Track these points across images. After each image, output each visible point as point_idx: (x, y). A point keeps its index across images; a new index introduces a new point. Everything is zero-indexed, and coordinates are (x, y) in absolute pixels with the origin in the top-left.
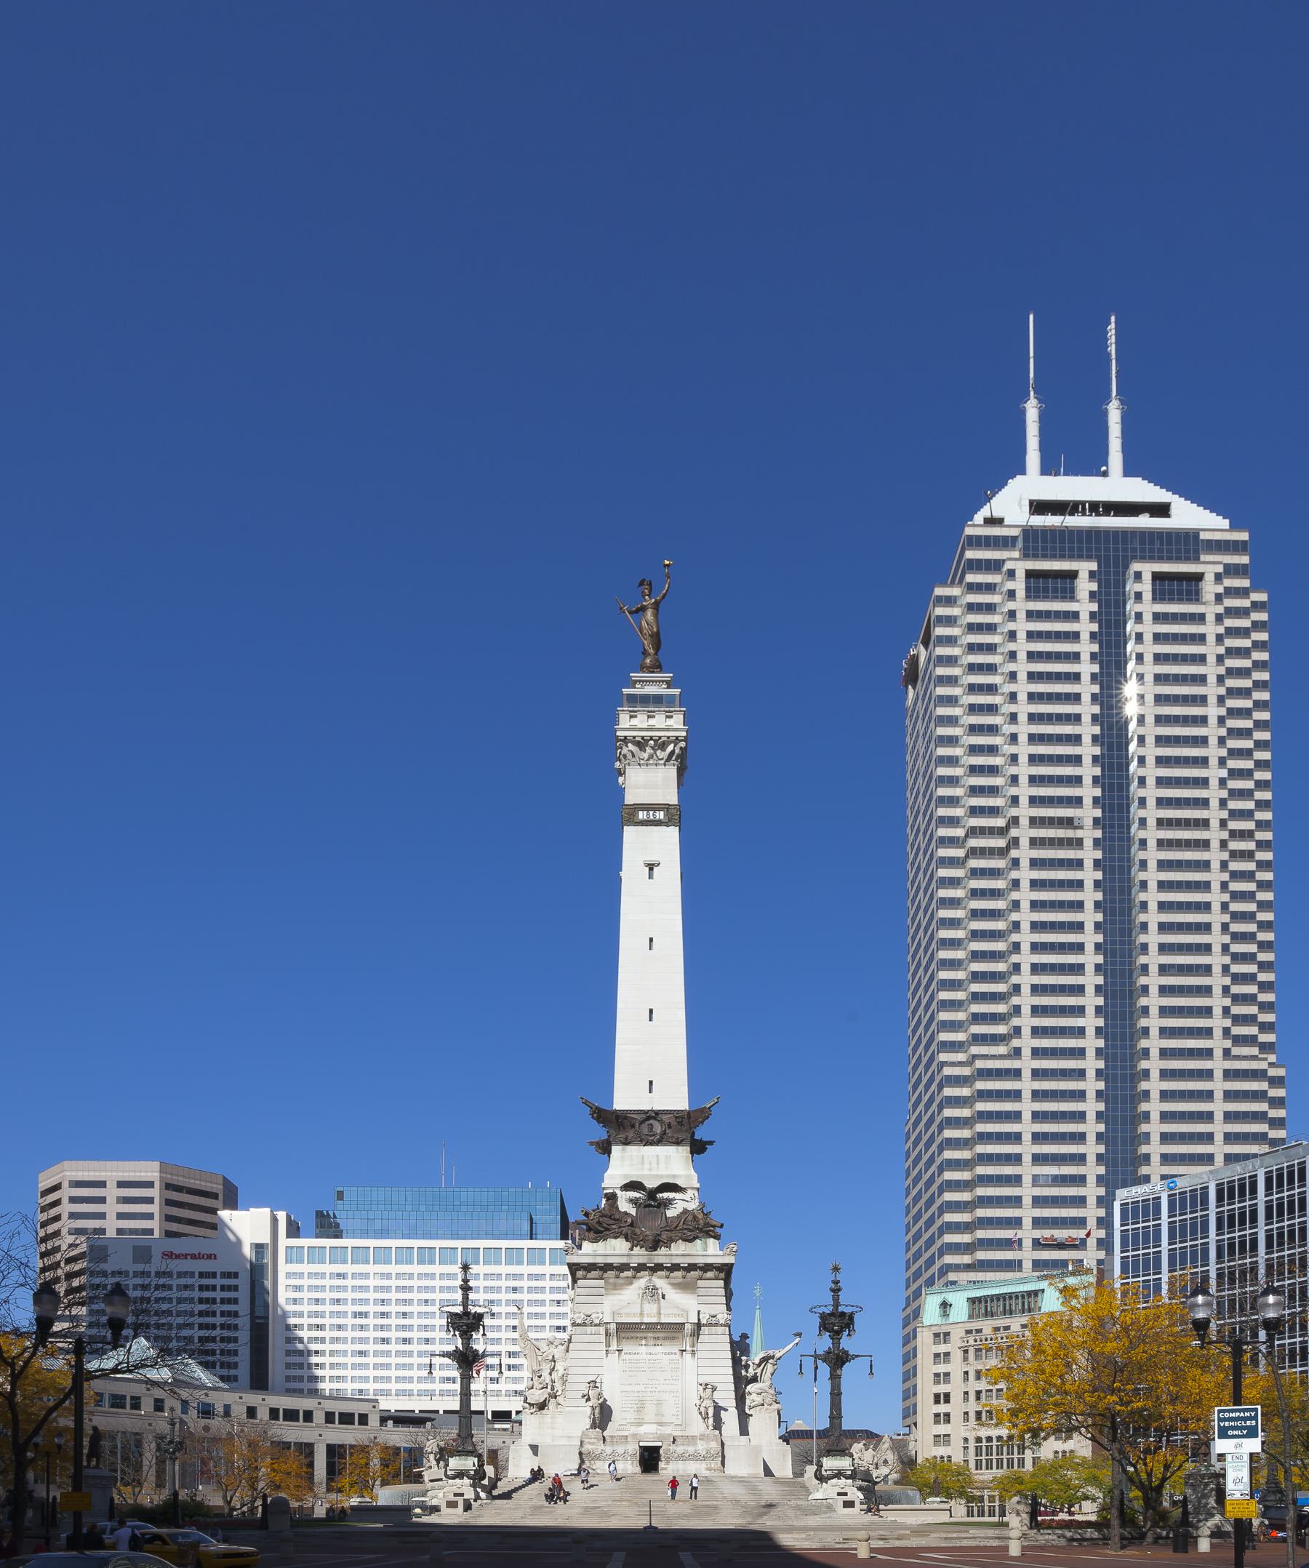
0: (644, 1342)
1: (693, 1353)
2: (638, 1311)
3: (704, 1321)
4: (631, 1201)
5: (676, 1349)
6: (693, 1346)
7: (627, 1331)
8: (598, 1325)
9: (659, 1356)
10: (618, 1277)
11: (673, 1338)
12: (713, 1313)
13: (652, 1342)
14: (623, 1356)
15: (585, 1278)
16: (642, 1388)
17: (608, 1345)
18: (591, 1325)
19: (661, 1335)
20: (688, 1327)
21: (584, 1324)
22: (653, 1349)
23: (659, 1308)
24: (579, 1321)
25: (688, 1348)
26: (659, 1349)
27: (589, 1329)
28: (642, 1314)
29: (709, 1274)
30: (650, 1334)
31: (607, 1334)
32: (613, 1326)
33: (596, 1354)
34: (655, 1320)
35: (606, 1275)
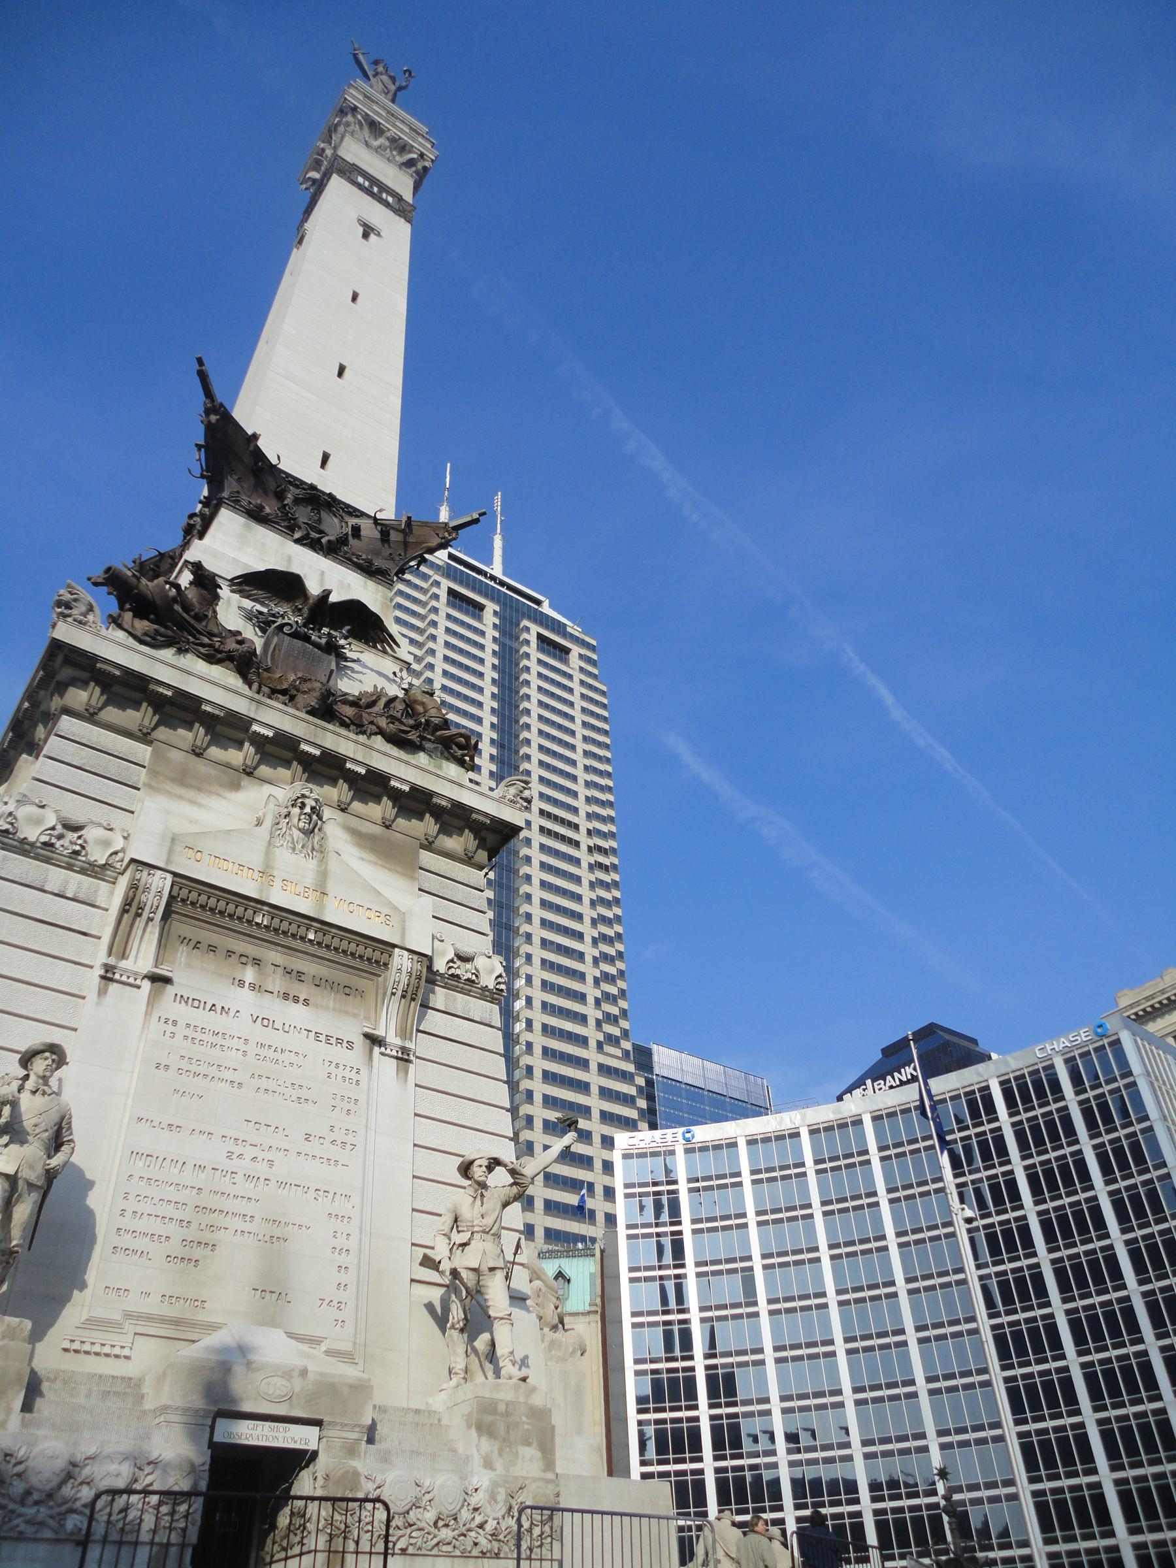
0: (249, 975)
1: (404, 1058)
2: (256, 859)
3: (440, 965)
4: (249, 616)
5: (353, 1031)
6: (403, 1033)
7: (202, 912)
8: (95, 871)
9: (294, 1041)
10: (198, 753)
11: (348, 990)
12: (467, 950)
13: (277, 982)
14: (168, 1004)
15: (90, 716)
16: (213, 1152)
17: (120, 946)
18: (76, 862)
19: (311, 968)
20: (401, 962)
21: (44, 852)
22: (274, 1008)
23: (323, 876)
24: (32, 834)
25: (393, 1039)
26: (297, 1014)
27: (56, 877)
28: (266, 873)
29: (452, 843)
30: (273, 955)
31: (131, 907)
32: (161, 884)
33: (60, 975)
34: (304, 906)
35: (163, 733)
